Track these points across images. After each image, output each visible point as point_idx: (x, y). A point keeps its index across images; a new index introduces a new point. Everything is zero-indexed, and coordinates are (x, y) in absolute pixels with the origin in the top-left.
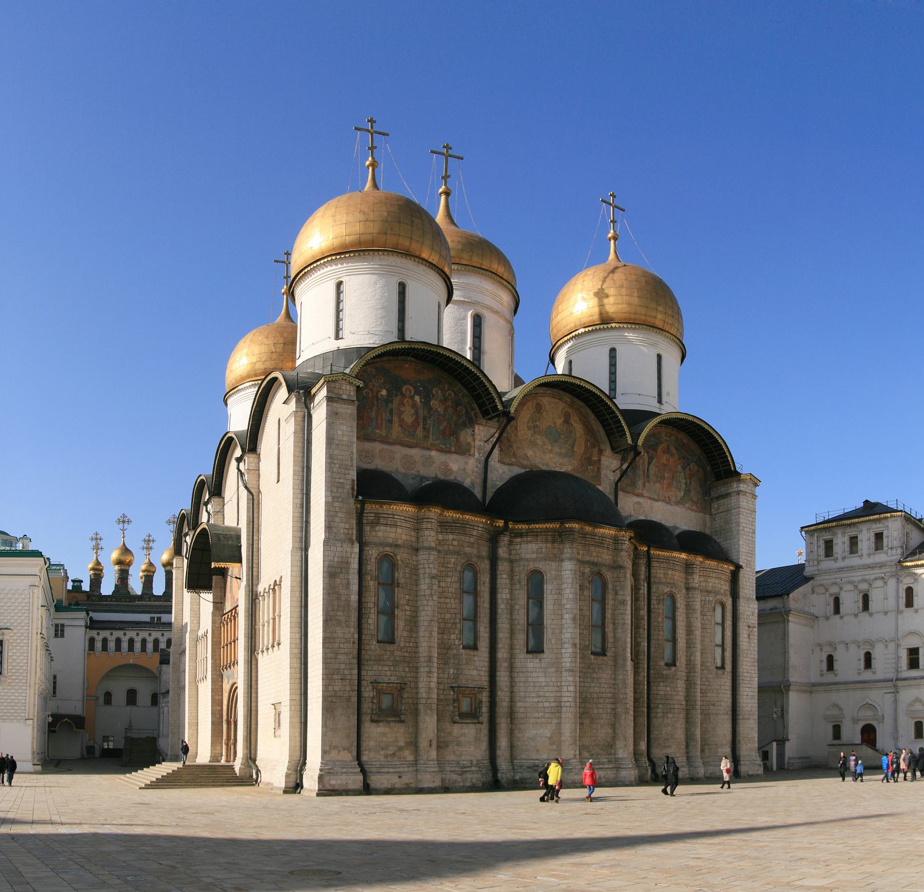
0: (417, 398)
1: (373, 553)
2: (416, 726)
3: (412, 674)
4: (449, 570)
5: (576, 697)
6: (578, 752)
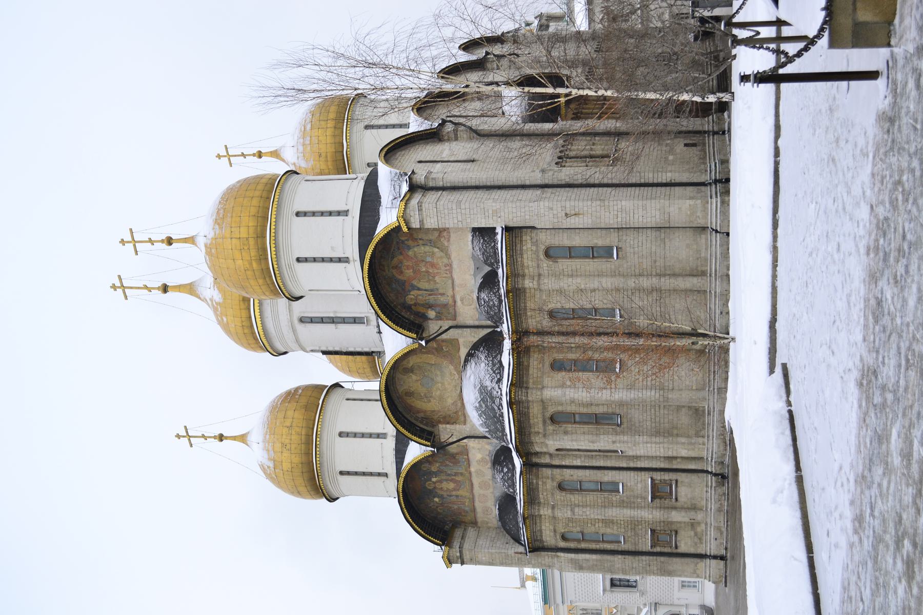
0: (434, 480)
1: (562, 544)
2: (680, 522)
3: (643, 522)
4: (565, 499)
5: (655, 443)
6: (701, 440)
